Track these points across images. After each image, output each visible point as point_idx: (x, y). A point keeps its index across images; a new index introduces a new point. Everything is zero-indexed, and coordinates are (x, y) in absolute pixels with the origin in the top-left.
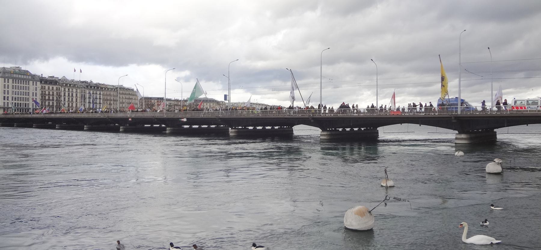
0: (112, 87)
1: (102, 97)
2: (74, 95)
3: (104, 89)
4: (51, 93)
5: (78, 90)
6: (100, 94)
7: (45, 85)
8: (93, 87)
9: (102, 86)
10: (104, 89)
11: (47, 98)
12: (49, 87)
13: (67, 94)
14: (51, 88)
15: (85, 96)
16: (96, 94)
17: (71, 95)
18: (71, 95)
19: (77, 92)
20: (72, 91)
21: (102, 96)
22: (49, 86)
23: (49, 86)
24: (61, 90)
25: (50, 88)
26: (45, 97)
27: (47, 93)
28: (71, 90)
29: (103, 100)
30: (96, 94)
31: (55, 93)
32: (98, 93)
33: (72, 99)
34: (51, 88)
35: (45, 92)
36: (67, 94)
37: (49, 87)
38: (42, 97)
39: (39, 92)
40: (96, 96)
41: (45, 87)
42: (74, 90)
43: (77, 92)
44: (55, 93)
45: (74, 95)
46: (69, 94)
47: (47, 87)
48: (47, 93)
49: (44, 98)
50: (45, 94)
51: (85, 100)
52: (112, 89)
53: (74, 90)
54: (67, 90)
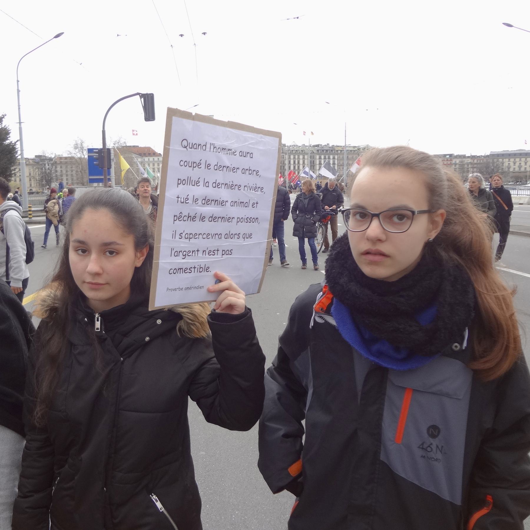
0: (352, 149)
1: (336, 162)
2: (301, 162)
3: (339, 152)
5: (306, 157)
6: (334, 158)
9: (337, 149)
10: (339, 152)
13: (292, 162)
15: (315, 163)
16: (328, 158)
17: (296, 162)
18: (296, 162)
19: (304, 158)
20: (299, 158)
24: (285, 158)
28: (296, 157)
29: (338, 165)
30: (329, 158)
32: (331, 157)
33: (299, 167)
36: (292, 162)
40: (329, 161)
42: (301, 157)
43: (304, 158)
45: (301, 162)
46: (294, 162)
51: (315, 166)
52: (351, 151)
53: (301, 157)
54: (292, 157)
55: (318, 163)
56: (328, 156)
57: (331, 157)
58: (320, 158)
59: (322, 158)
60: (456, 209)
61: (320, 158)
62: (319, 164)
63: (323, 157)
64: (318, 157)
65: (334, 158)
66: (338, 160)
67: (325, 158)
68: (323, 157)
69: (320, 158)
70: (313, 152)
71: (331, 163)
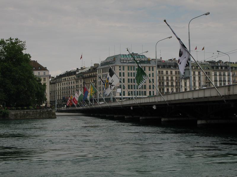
2: (197, 79)
4: (170, 78)
5: (202, 73)
7: (162, 70)
8: (220, 68)
11: (165, 84)
12: (167, 72)
14: (169, 72)
21: (231, 78)
22: (167, 70)
23: (167, 70)
25: (168, 72)
26: (163, 83)
27: (165, 78)
30: (224, 75)
31: (174, 78)
32: (226, 74)
34: (169, 72)
35: (163, 77)
37: (167, 72)
38: (160, 83)
39: (156, 79)
41: (162, 71)
42: (197, 73)
44: (174, 78)
45: (197, 79)
47: (165, 72)
48: (165, 78)
49: (161, 84)
50: (163, 79)
53: (197, 73)
55: (213, 80)
56: (223, 73)
57: (226, 74)
58: (215, 75)
59: (217, 75)
60: (68, 173)
61: (216, 75)
62: (215, 80)
63: (218, 74)
64: (213, 73)
65: (229, 75)
66: (233, 77)
67: (220, 75)
68: (218, 74)
69: (215, 75)
70: (208, 69)
71: (226, 80)
